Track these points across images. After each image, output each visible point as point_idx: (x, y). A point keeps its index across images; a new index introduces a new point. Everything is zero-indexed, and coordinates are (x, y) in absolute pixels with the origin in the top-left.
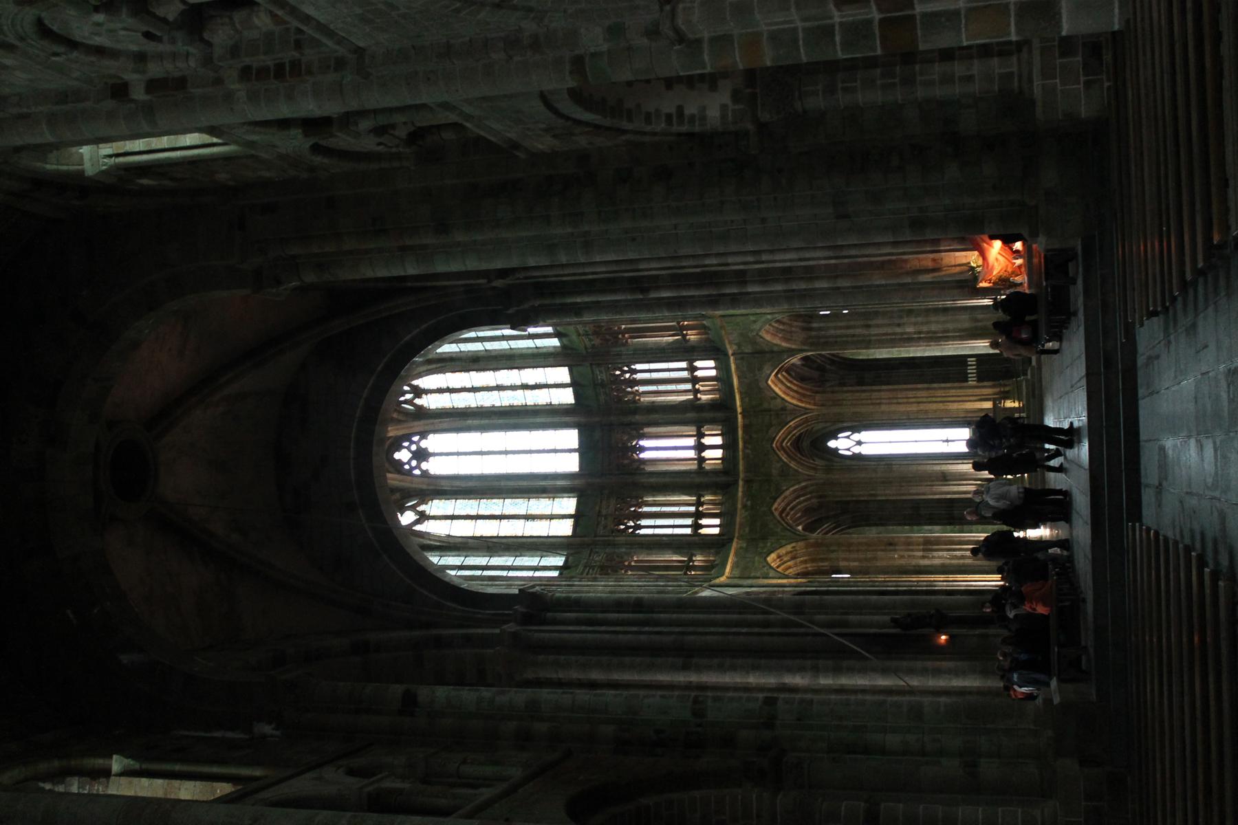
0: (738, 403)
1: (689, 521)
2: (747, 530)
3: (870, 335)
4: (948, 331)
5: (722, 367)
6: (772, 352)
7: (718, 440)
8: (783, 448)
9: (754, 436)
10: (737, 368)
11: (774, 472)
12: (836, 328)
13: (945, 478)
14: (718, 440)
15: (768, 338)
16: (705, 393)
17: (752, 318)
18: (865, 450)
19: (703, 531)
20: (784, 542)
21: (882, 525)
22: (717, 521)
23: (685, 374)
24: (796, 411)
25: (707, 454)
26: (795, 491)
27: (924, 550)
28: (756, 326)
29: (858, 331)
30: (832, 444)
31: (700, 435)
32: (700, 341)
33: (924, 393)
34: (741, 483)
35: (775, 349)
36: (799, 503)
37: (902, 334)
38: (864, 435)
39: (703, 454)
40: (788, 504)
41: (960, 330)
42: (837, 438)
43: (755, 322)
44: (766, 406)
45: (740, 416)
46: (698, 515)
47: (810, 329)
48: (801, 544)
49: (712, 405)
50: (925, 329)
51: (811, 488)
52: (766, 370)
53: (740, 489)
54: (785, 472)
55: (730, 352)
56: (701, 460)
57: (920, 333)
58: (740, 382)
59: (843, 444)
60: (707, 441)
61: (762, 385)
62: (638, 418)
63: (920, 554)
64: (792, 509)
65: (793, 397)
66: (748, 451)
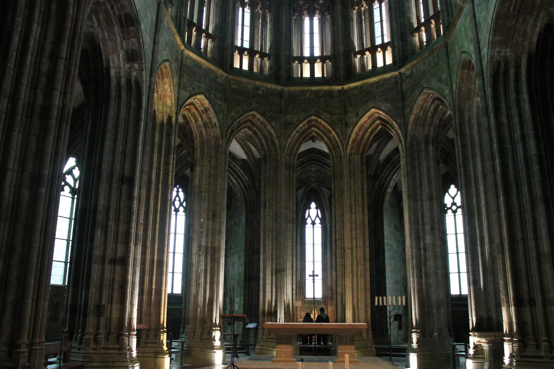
0: (352, 85)
1: (246, 45)
2: (235, 87)
3: (422, 200)
4: (427, 277)
5: (386, 69)
6: (404, 108)
7: (318, 74)
9: (322, 99)
10: (386, 80)
11: (288, 117)
12: (428, 168)
13: (279, 272)
14: (318, 74)
15: (420, 101)
16: (362, 59)
17: (444, 76)
18: (308, 228)
19: (237, 57)
20: (221, 116)
22: (245, 67)
23: (378, 42)
24: (344, 136)
25: (307, 67)
26: (271, 134)
27: (207, 247)
28: (434, 83)
29: (426, 188)
30: (313, 205)
31: (323, 59)
32: (413, 45)
33: (360, 254)
34: (279, 88)
35: (407, 110)
36: (260, 140)
37: (424, 231)
38: (318, 228)
39: (306, 61)
41: (427, 290)
43: (440, 80)
44: (350, 109)
45: (340, 87)
46: (251, 52)
47: (427, 145)
48: (218, 131)
49: (350, 67)
50: (430, 254)
51: (273, 149)
52: (387, 106)
53: (273, 86)
54: (289, 126)
55: (403, 70)
56: (301, 59)
57: (425, 249)
58: (372, 84)
59: (313, 212)
60: (318, 67)
61: (370, 104)
62: (339, 7)
63: (203, 244)
64: (255, 132)
65: (357, 134)
66: (308, 94)
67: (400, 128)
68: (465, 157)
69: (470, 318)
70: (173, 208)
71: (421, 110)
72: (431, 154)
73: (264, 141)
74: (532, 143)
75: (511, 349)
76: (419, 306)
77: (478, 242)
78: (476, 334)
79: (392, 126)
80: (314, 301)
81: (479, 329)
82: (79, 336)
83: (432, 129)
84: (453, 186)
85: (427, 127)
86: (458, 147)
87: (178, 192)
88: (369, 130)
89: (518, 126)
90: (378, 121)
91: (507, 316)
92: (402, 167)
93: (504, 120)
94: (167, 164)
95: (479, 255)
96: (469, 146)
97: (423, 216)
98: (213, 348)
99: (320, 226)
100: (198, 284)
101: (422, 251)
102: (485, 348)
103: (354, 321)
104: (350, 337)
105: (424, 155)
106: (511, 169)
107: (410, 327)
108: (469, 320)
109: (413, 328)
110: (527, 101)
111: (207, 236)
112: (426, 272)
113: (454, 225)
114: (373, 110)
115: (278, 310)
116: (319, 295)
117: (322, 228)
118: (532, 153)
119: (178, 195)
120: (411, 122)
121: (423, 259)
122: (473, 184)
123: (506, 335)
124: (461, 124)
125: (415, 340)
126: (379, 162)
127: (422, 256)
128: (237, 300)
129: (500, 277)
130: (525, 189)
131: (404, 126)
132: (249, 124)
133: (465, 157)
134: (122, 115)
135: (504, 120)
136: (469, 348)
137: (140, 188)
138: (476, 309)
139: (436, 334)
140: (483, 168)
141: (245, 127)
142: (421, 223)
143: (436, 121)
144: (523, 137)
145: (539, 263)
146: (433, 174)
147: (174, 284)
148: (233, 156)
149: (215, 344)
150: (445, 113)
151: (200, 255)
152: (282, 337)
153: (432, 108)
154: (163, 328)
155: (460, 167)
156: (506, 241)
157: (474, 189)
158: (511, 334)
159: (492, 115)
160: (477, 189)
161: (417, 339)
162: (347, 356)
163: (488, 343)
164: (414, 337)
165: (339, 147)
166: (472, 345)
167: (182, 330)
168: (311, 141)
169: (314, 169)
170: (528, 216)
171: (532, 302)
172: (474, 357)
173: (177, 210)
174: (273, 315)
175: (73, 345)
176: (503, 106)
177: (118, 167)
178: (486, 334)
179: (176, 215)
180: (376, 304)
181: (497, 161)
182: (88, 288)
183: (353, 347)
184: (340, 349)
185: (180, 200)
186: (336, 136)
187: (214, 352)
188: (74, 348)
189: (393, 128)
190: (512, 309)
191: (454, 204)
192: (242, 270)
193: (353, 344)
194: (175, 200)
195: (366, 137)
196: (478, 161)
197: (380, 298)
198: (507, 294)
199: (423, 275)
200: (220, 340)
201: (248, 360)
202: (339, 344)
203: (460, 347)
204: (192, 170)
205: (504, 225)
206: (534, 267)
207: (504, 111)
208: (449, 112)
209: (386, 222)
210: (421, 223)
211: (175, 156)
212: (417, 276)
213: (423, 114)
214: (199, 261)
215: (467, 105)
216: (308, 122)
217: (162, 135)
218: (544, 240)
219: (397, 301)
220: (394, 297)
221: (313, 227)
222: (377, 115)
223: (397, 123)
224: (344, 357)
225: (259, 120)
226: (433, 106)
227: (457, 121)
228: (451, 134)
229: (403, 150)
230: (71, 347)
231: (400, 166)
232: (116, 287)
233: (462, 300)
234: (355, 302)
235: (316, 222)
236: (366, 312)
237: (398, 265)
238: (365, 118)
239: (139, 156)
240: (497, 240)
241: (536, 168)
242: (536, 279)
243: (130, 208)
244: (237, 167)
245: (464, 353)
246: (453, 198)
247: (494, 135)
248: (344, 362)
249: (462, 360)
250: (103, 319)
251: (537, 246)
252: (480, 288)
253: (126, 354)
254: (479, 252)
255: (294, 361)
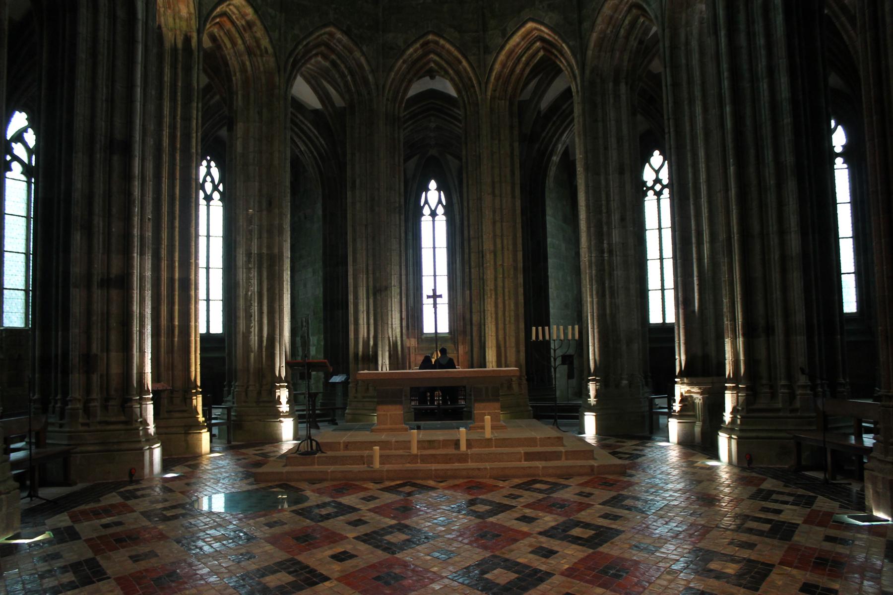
4: (612, 295)
6: (580, 23)
8: (426, 54)
13: (379, 292)
18: (426, 222)
21: (324, 216)
26: (360, 66)
27: (260, 255)
29: (613, 154)
30: (433, 185)
35: (586, 25)
36: (343, 76)
37: (609, 224)
38: (441, 221)
40: (339, 56)
42: (439, 189)
47: (616, 82)
48: (272, 60)
50: (618, 260)
57: (610, 252)
59: (433, 195)
63: (255, 250)
65: (504, 65)
67: (574, 54)
68: (677, 103)
69: (677, 357)
70: (202, 195)
71: (609, 24)
72: (624, 98)
73: (349, 78)
74: (783, 80)
75: (735, 401)
76: (600, 341)
77: (694, 240)
78: (685, 380)
79: (561, 52)
80: (436, 337)
81: (690, 373)
82: (59, 405)
83: (626, 57)
84: (656, 153)
85: (617, 54)
86: (666, 86)
87: (209, 167)
88: (524, 59)
89: (763, 52)
90: (538, 44)
91: (732, 351)
92: (576, 121)
93: (742, 40)
94: (187, 119)
95: (695, 261)
96: (685, 85)
97: (608, 201)
98: (277, 415)
99: (444, 218)
100: (249, 316)
101: (606, 255)
102: (697, 401)
103: (499, 364)
104: (492, 389)
105: (612, 101)
106: (749, 122)
107: (586, 373)
108: (675, 359)
109: (590, 374)
110: (780, 10)
111: (260, 237)
112: (611, 288)
113: (657, 215)
114: (530, 25)
115: (380, 353)
116: (444, 328)
117: (447, 221)
118: (783, 96)
119: (209, 173)
120: (592, 45)
121: (607, 267)
122: (688, 148)
123: (729, 380)
124: (674, 48)
125: (592, 393)
126: (539, 112)
127: (606, 262)
128: (313, 340)
129: (724, 292)
130: (769, 155)
131: (580, 51)
132: (323, 48)
133: (677, 103)
134: (103, 34)
135: (742, 40)
136: (674, 401)
137: (143, 160)
138: (686, 343)
139: (625, 382)
140: (706, 121)
141: (316, 55)
142: (604, 211)
143: (633, 43)
144: (771, 72)
145: (784, 271)
146: (625, 131)
147: (210, 317)
148: (298, 105)
149: (281, 410)
150: (648, 30)
151: (249, 270)
152: (386, 392)
153: (627, 22)
154: (196, 387)
155: (669, 119)
156: (736, 237)
157: (689, 155)
158: (736, 378)
159: (723, 33)
160: (695, 155)
161: (597, 391)
162: (488, 418)
163: (701, 394)
164: (592, 388)
165: (473, 86)
166: (678, 398)
167: (226, 389)
168: (428, 78)
169: (433, 125)
170: (771, 198)
171: (769, 330)
172: (681, 415)
173: (208, 198)
174: (371, 360)
175: (51, 420)
176: (742, 17)
177: (101, 124)
178: (700, 379)
179: (208, 206)
180: (534, 338)
181: (728, 109)
182: (66, 328)
183: (497, 405)
184: (478, 409)
185: (213, 181)
186: (469, 69)
187: (281, 422)
188: (53, 424)
189: (562, 55)
190: (740, 341)
191: (657, 181)
192: (319, 291)
193: (498, 401)
194: (205, 181)
195: (518, 70)
196: (699, 109)
197: (540, 328)
198: (733, 319)
199: (607, 293)
200: (287, 403)
201: (334, 430)
202: (476, 401)
203: (661, 402)
204: (231, 129)
205: (734, 211)
206: (776, 276)
207: (742, 27)
208: (654, 29)
209: (549, 211)
210: (604, 211)
211: (200, 105)
212: (597, 293)
213: (612, 32)
214: (248, 279)
215: (684, 15)
216: (422, 46)
217: (176, 68)
218: (793, 235)
219: (565, 334)
220: (561, 328)
221: (434, 221)
222: (536, 33)
223: (569, 47)
224: (483, 421)
225: (339, 41)
226: (629, 18)
227: (667, 44)
228: (656, 66)
229: (578, 92)
230: (47, 424)
231: (572, 120)
232: (114, 323)
233: (666, 330)
234: (501, 337)
235: (438, 212)
236: (518, 352)
237: (569, 279)
238: (516, 39)
239: (138, 106)
240: (722, 236)
241: (787, 120)
242: (777, 294)
243: (129, 194)
244: (306, 122)
245: (666, 410)
246: (657, 172)
247: (725, 66)
248: (483, 428)
249: (662, 420)
250: (95, 378)
251: (783, 244)
252: (694, 311)
253: (137, 429)
254: (695, 255)
255: (406, 430)
